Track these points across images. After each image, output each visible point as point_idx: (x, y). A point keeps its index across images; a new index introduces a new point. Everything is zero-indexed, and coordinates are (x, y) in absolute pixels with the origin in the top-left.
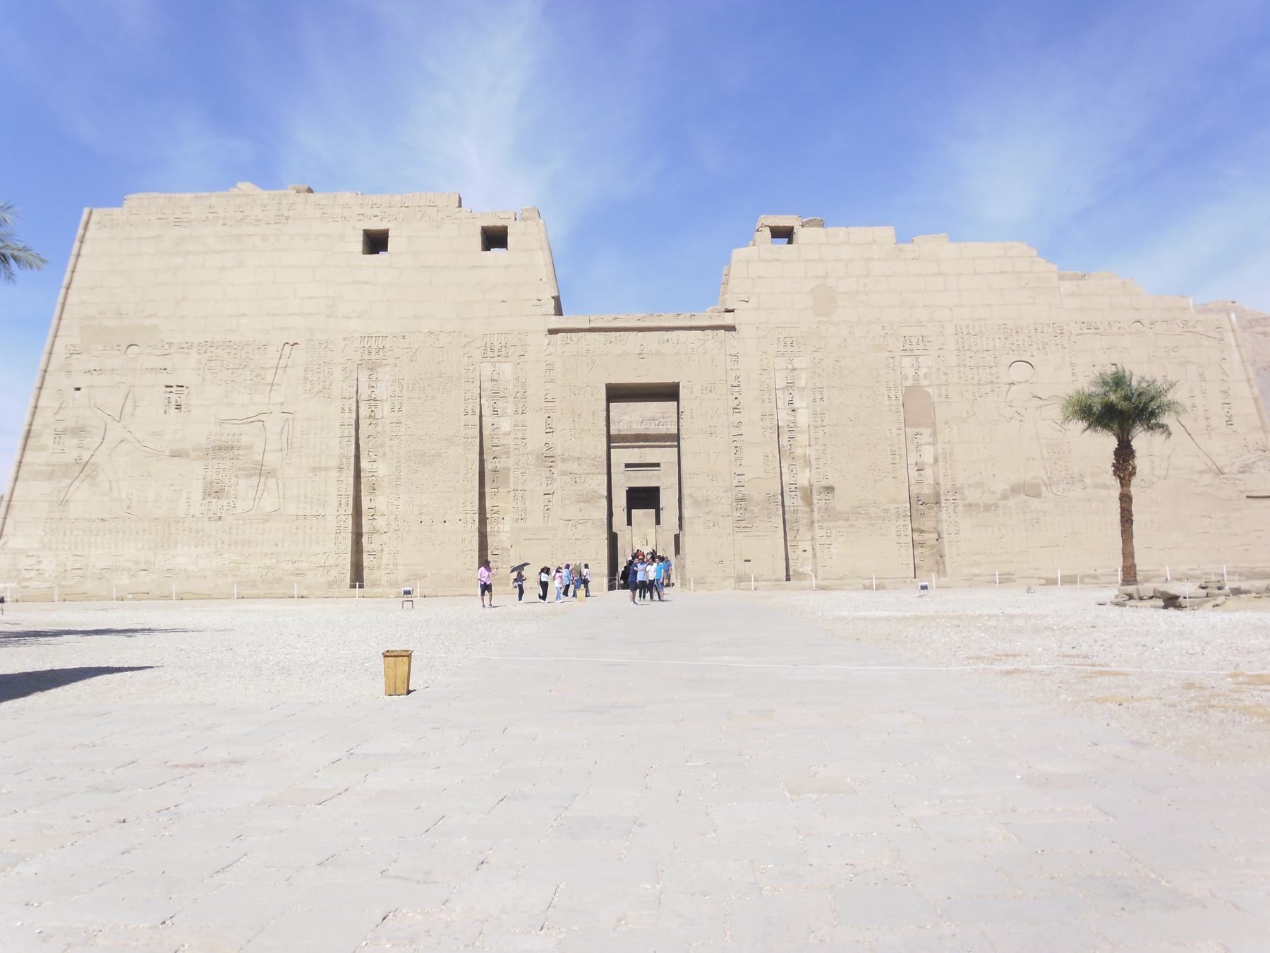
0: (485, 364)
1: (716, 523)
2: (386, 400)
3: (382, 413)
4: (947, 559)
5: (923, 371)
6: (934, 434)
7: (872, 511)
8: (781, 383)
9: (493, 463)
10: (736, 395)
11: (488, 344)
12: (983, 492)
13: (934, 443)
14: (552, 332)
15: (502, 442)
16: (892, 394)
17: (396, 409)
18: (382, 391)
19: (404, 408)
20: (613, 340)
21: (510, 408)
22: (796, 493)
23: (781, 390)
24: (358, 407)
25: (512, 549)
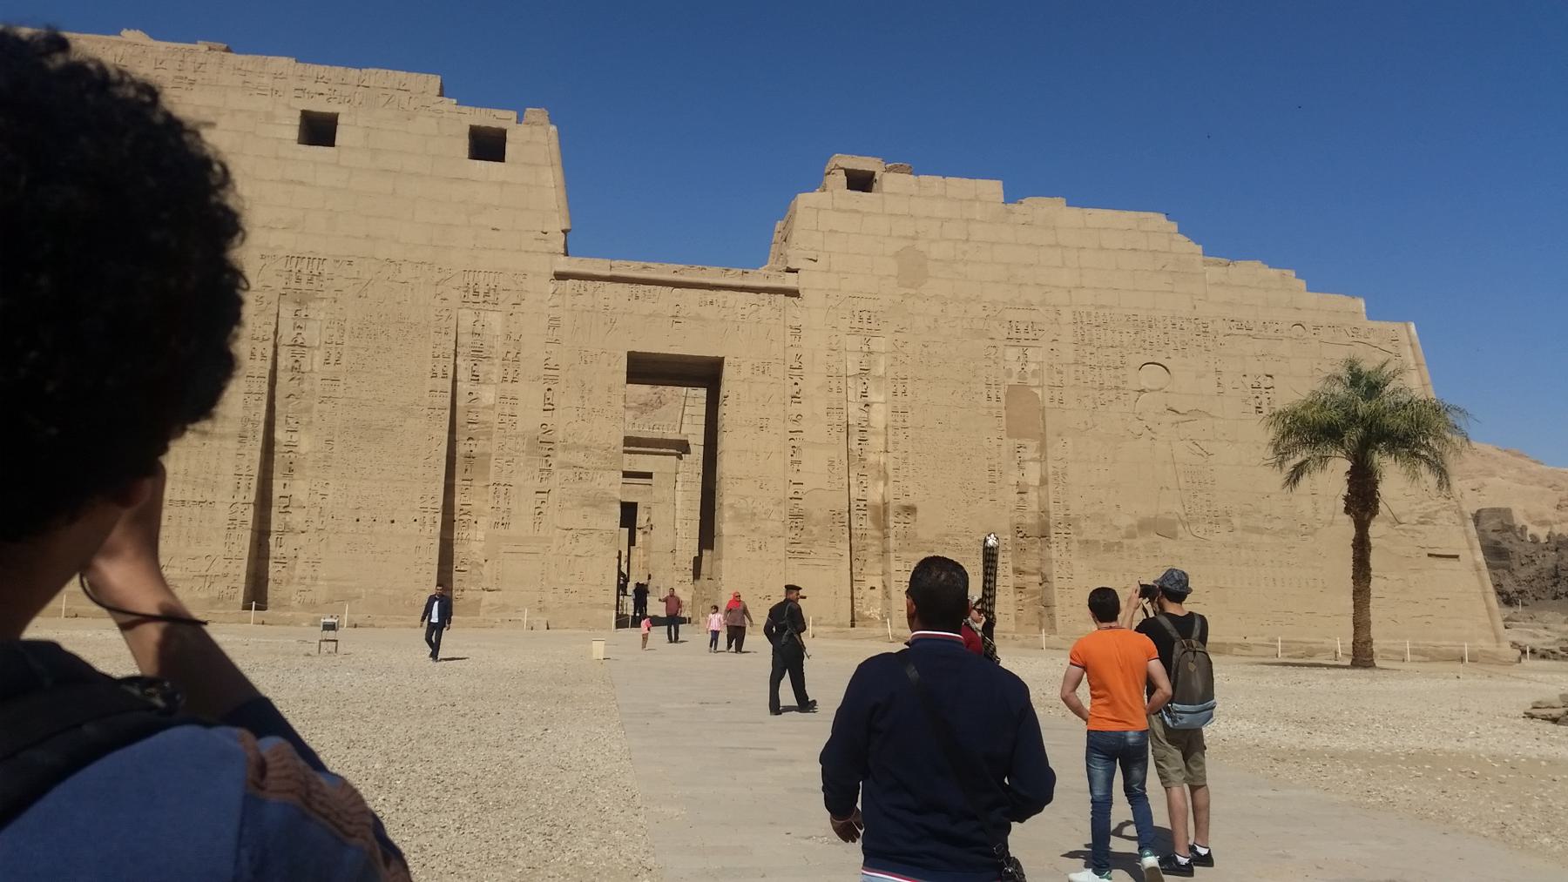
0: (466, 311)
1: (763, 544)
2: (318, 348)
3: (312, 365)
4: (1058, 611)
5: (1032, 367)
6: (1042, 448)
7: (963, 541)
8: (853, 369)
9: (467, 446)
10: (796, 379)
11: (472, 284)
12: (1104, 526)
13: (1042, 460)
14: (561, 276)
15: (482, 418)
16: (993, 394)
17: (332, 360)
18: (311, 334)
19: (343, 360)
20: (640, 294)
21: (496, 373)
22: (865, 512)
23: (852, 378)
24: (275, 353)
25: (486, 566)
